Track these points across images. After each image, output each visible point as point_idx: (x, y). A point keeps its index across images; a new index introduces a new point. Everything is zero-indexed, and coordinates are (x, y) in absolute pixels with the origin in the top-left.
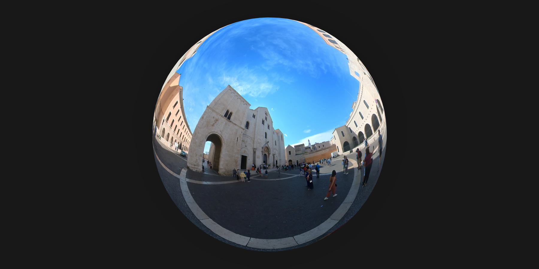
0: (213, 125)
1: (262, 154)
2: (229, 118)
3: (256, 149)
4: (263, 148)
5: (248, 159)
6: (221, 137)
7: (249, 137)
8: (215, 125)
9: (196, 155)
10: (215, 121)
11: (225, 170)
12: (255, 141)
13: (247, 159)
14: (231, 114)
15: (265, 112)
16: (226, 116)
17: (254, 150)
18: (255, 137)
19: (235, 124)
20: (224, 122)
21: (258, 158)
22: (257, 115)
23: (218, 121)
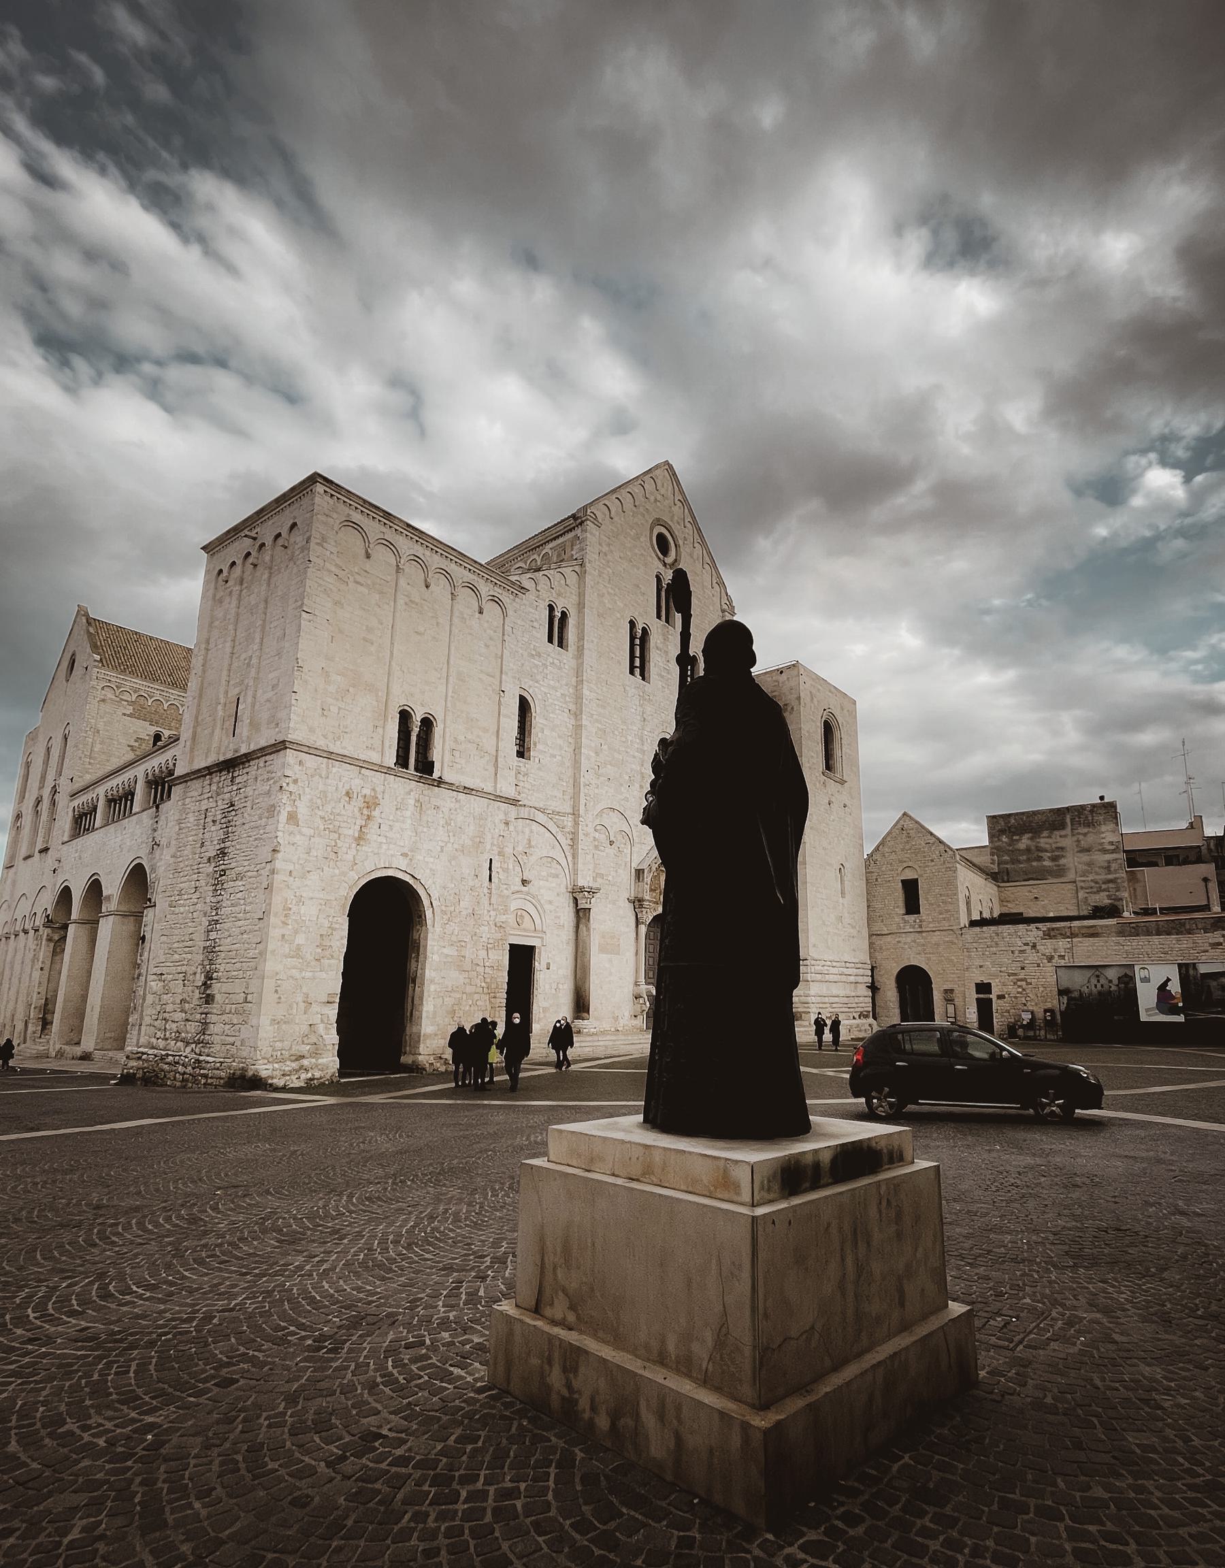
0: (360, 839)
2: (425, 767)
3: (592, 892)
4: (639, 873)
6: (411, 881)
7: (541, 817)
8: (372, 833)
10: (360, 809)
12: (581, 836)
14: (427, 724)
17: (576, 900)
18: (582, 808)
19: (467, 790)
20: (412, 802)
21: (611, 948)
22: (581, 606)
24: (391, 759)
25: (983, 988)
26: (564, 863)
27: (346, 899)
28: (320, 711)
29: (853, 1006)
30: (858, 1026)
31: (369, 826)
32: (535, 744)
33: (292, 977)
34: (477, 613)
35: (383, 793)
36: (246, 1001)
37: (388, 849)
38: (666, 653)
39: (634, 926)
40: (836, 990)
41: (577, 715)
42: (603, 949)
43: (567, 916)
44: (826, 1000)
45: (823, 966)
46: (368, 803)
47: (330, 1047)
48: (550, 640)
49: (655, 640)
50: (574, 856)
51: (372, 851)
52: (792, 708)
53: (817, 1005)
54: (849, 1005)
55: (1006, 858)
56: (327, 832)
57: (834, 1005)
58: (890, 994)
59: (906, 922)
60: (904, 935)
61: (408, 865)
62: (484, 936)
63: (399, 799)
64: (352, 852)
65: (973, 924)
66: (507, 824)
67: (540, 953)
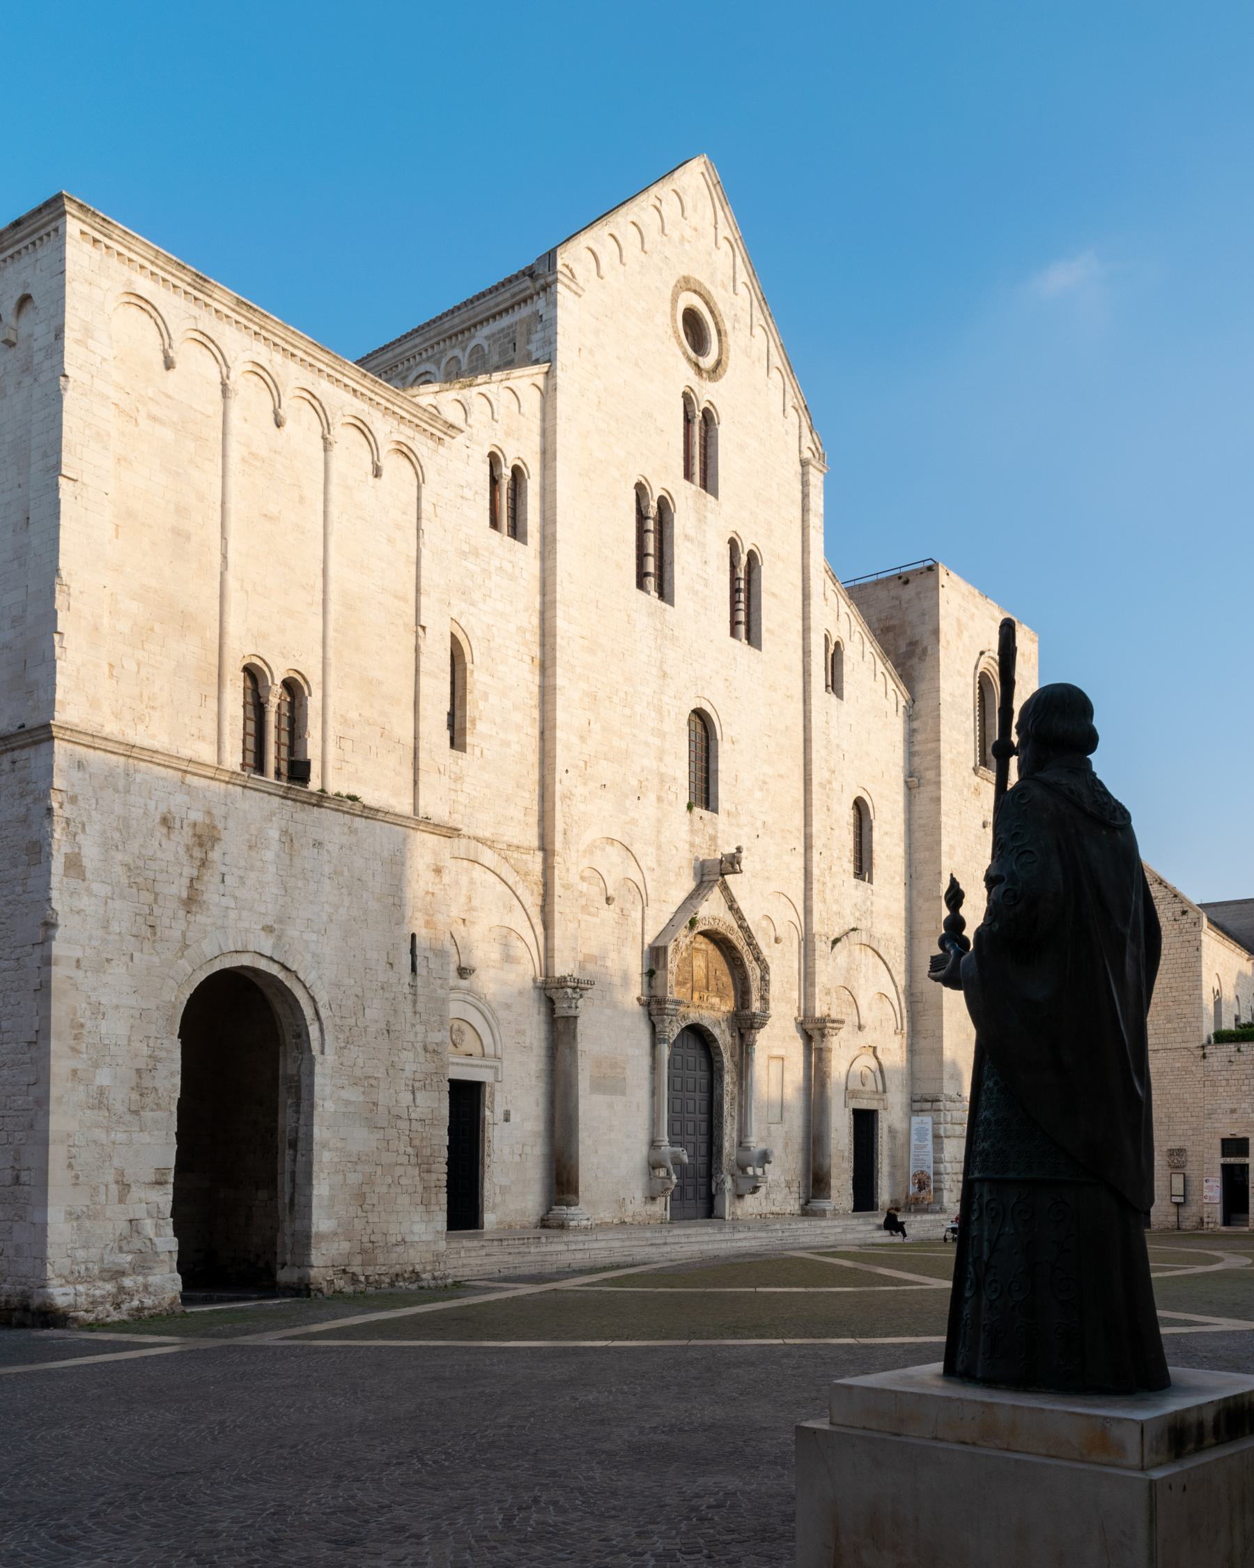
0: (192, 901)
2: (298, 771)
8: (211, 893)
9: (125, 1187)
17: (550, 1003)
20: (274, 834)
23: (215, 840)
27: (174, 1007)
28: (106, 669)
31: (205, 878)
32: (473, 722)
33: (95, 1142)
35: (225, 818)
36: (17, 1181)
37: (240, 919)
38: (702, 545)
47: (163, 1257)
50: (547, 925)
51: (213, 924)
56: (135, 890)
61: (274, 947)
62: (407, 1068)
63: (253, 830)
64: (180, 925)
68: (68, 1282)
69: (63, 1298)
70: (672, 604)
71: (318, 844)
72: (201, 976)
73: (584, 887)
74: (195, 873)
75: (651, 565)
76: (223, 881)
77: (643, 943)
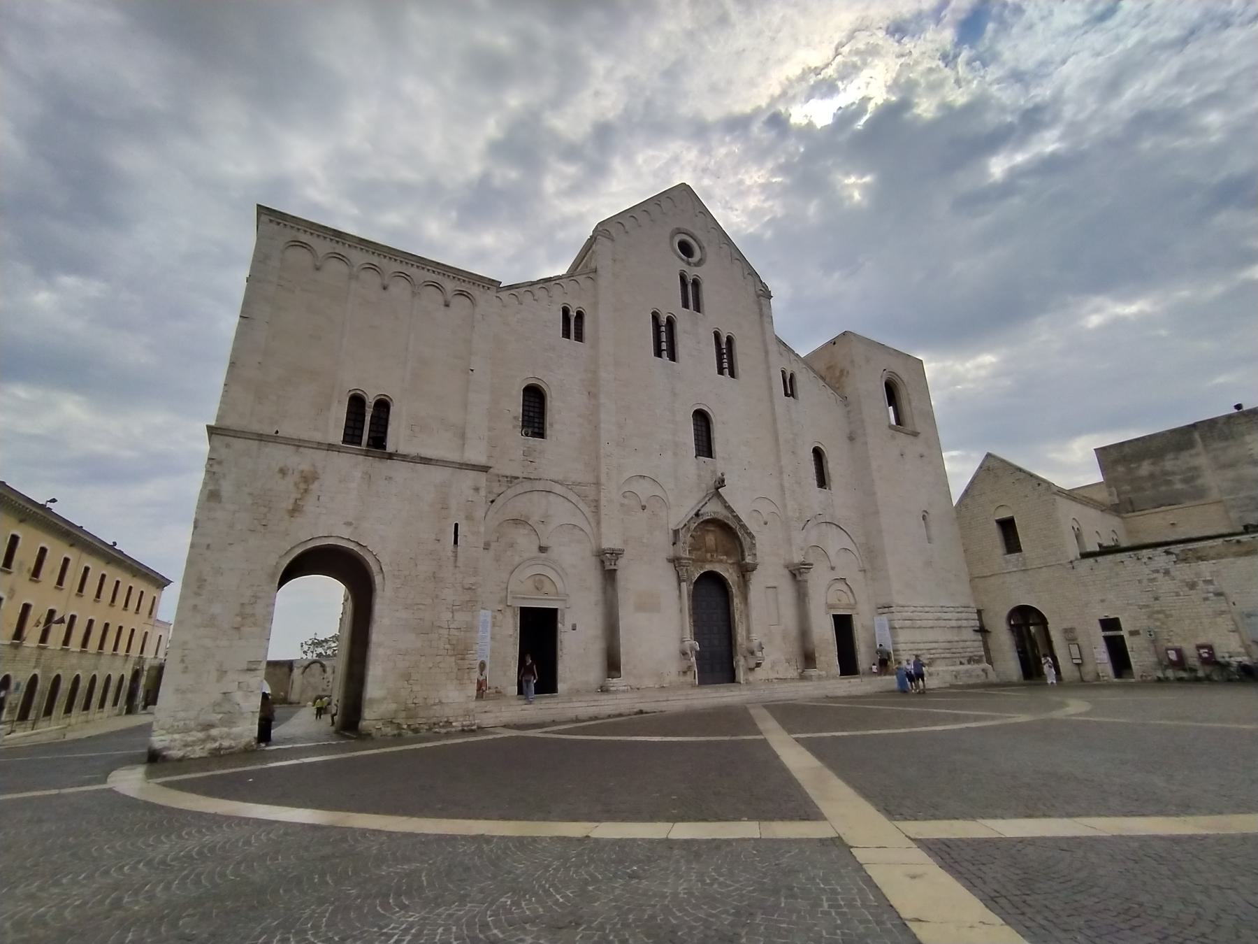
1: (680, 581)
2: (378, 442)
3: (616, 554)
4: (676, 532)
5: (568, 625)
6: (356, 549)
7: (558, 489)
8: (310, 505)
10: (296, 484)
11: (393, 706)
12: (603, 502)
13: (560, 625)
14: (383, 406)
15: (679, 231)
16: (352, 435)
17: (603, 562)
18: (603, 479)
20: (358, 474)
22: (595, 305)
24: (337, 436)
25: (1110, 624)
26: (587, 529)
29: (957, 651)
30: (967, 671)
32: (551, 425)
34: (443, 308)
39: (675, 584)
40: (931, 635)
41: (593, 395)
42: (640, 608)
43: (593, 579)
44: (922, 646)
45: (912, 612)
46: (305, 477)
48: (566, 334)
49: (679, 328)
50: (598, 523)
52: (848, 372)
53: (910, 652)
54: (954, 651)
55: (1127, 488)
57: (933, 651)
58: (1004, 640)
59: (1007, 562)
60: (1007, 575)
65: (1085, 555)
66: (477, 489)
67: (563, 616)
68: (169, 733)
69: (160, 743)
70: (678, 362)
71: (389, 478)
72: (299, 551)
73: (626, 501)
74: (299, 496)
75: (664, 346)
76: (319, 499)
77: (668, 529)
